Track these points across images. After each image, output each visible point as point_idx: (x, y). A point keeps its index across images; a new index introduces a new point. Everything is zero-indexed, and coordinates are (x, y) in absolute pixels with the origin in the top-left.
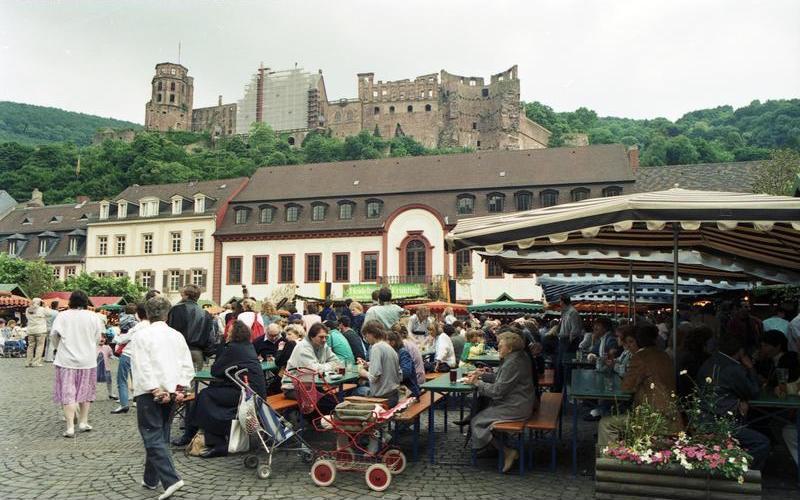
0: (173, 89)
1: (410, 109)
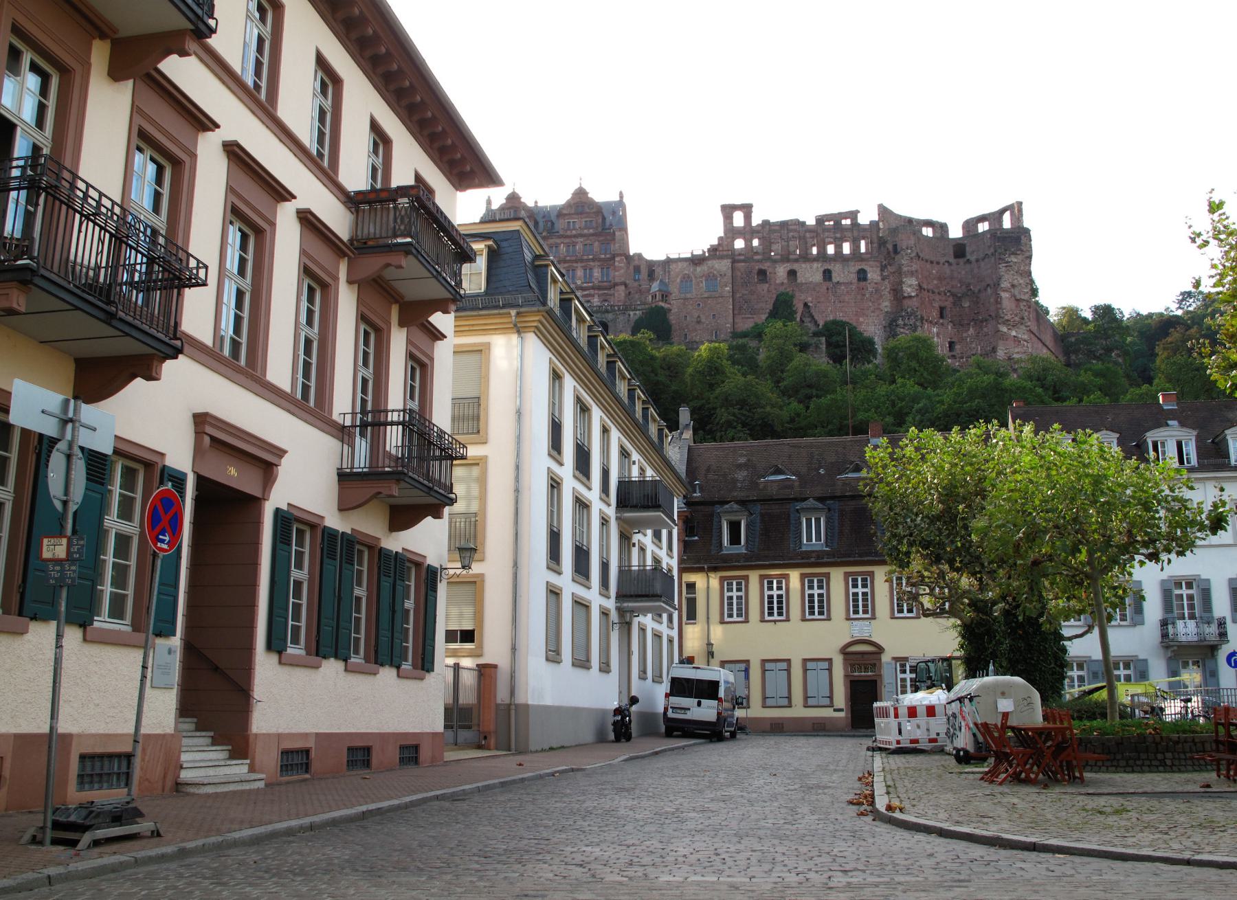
1: (827, 274)
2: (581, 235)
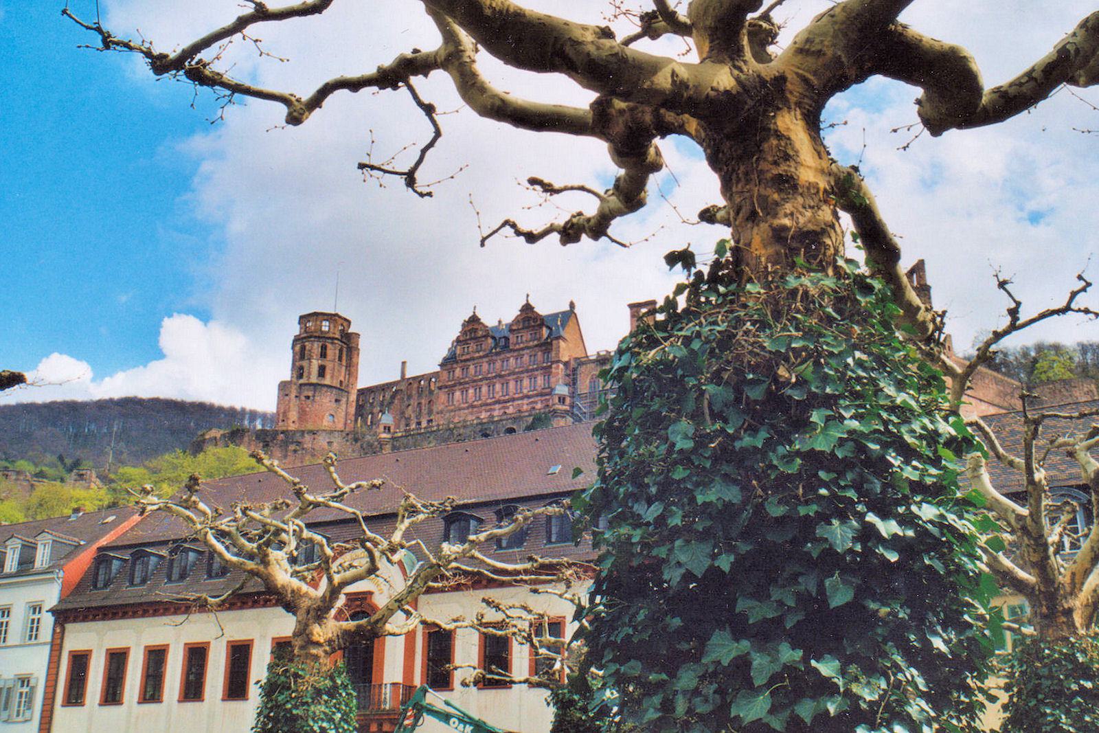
0: (323, 355)
2: (528, 348)
